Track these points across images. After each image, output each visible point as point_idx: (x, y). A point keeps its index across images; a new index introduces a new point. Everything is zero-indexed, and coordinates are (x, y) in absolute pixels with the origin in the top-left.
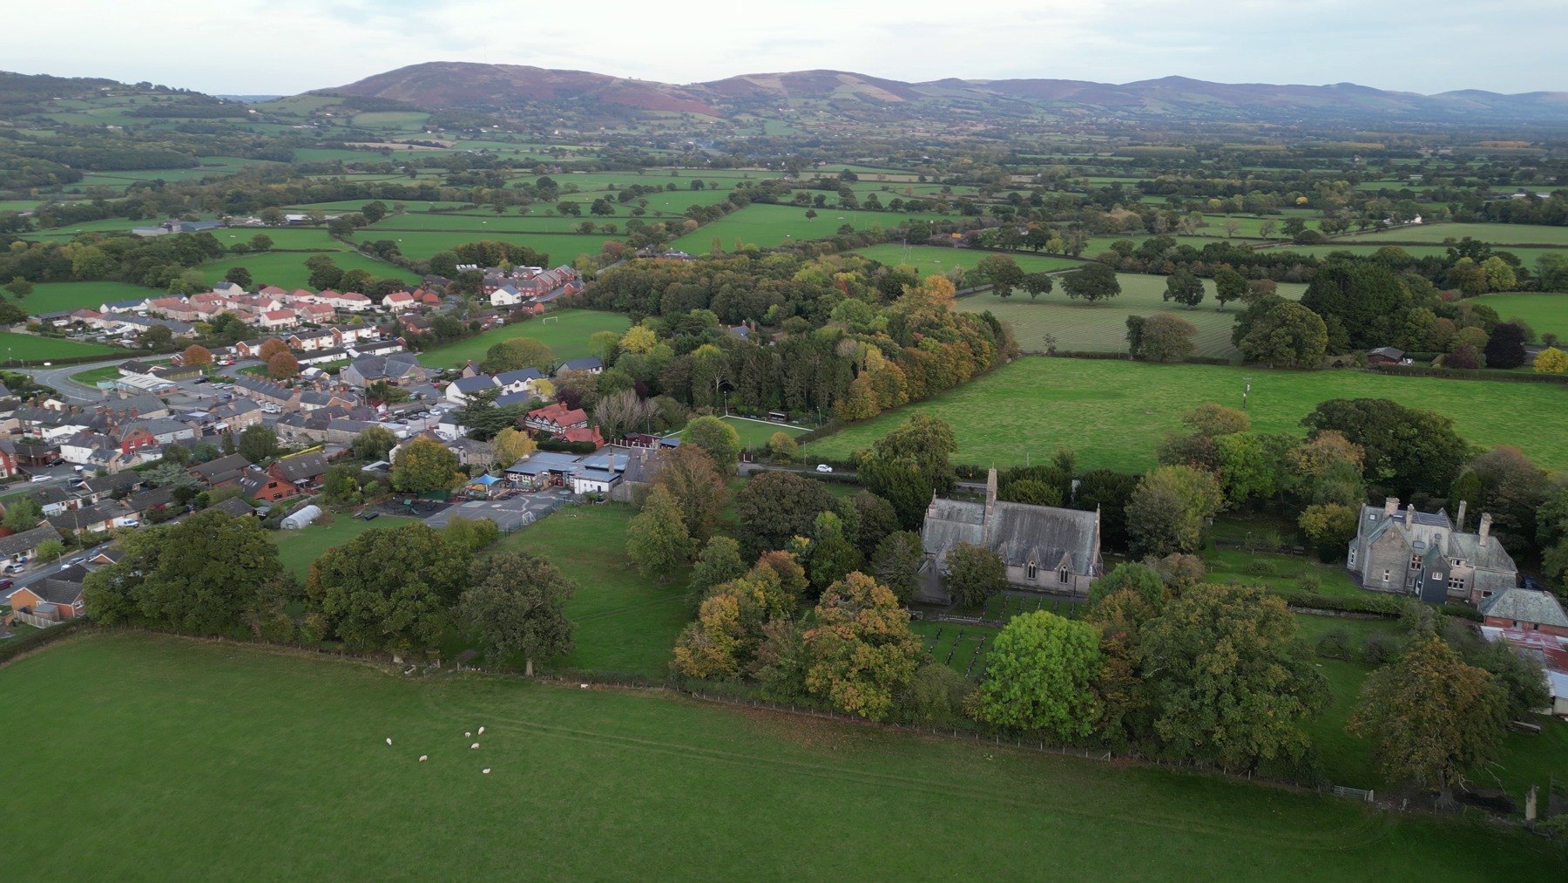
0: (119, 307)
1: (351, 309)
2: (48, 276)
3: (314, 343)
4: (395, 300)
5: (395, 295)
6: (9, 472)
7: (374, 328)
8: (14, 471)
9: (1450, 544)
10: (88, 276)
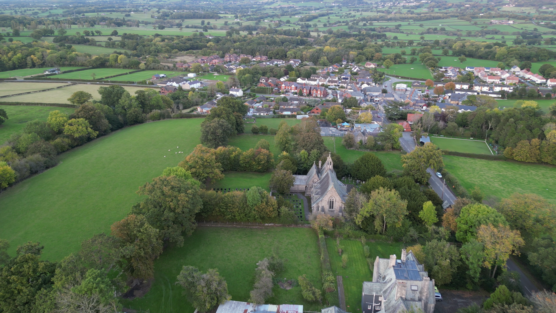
0: (470, 68)
1: (537, 82)
2: (489, 58)
3: (480, 88)
4: (551, 81)
5: (553, 79)
6: (321, 96)
7: (512, 88)
8: (322, 96)
9: (389, 287)
10: (498, 60)
